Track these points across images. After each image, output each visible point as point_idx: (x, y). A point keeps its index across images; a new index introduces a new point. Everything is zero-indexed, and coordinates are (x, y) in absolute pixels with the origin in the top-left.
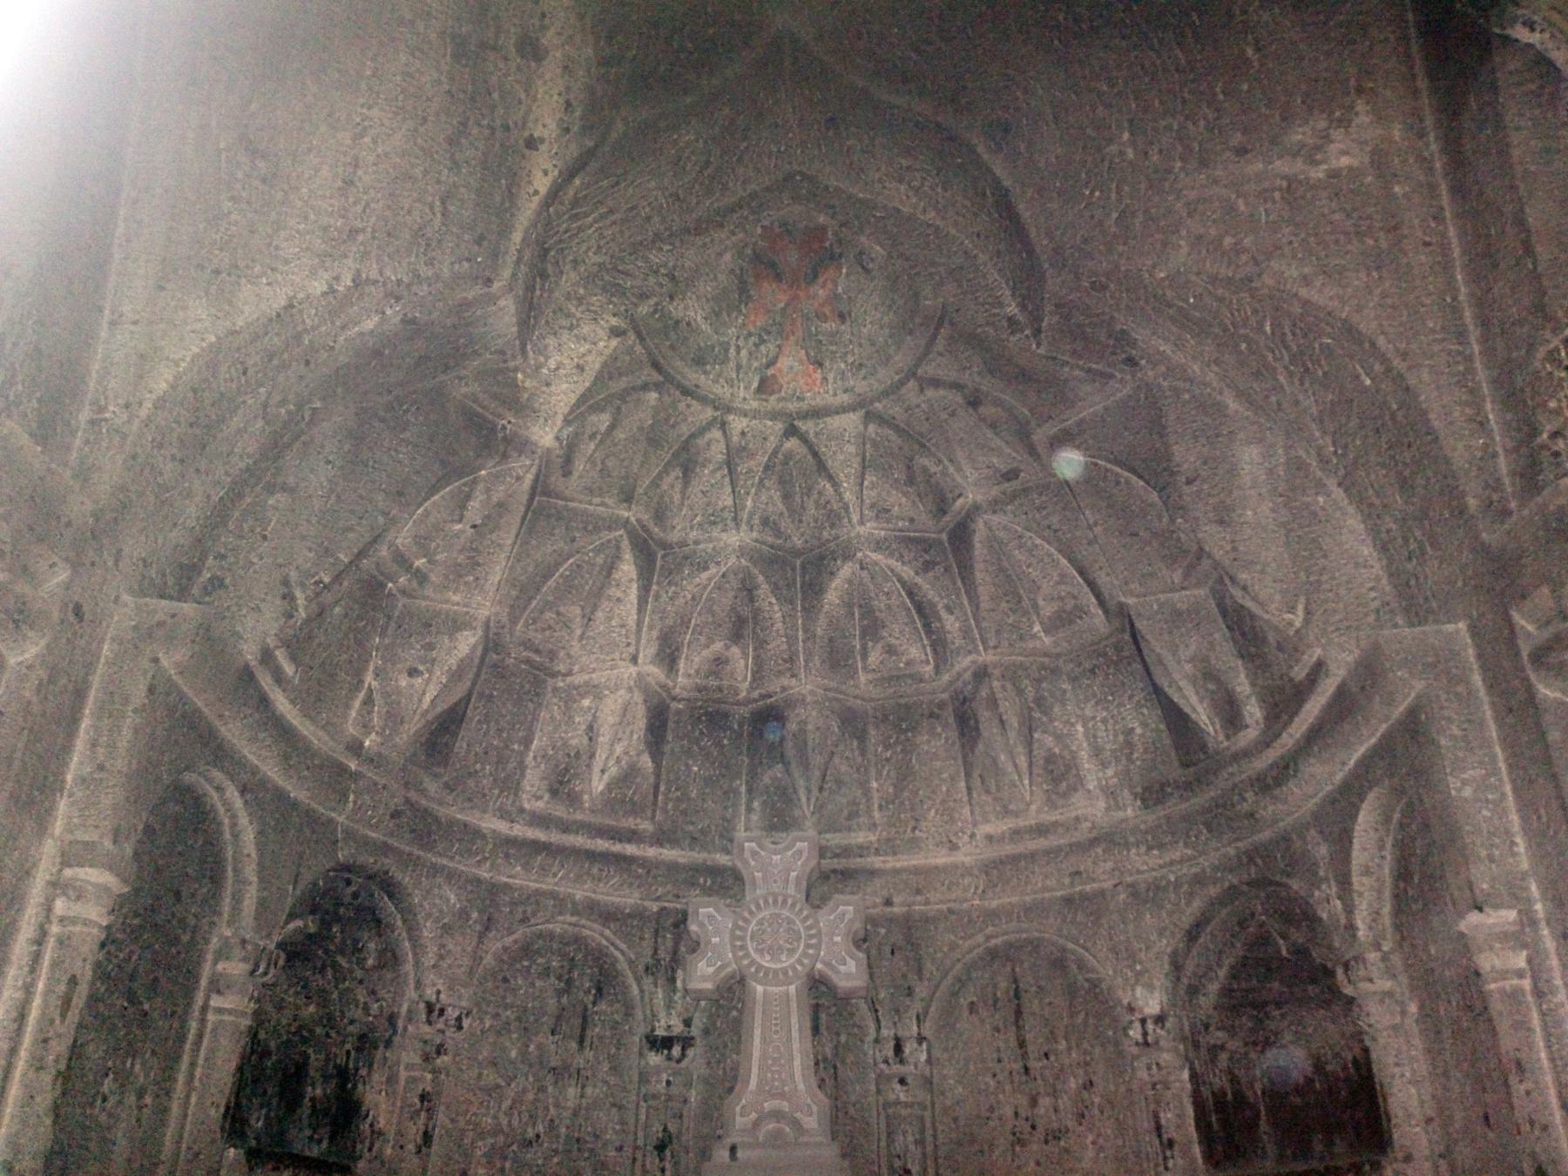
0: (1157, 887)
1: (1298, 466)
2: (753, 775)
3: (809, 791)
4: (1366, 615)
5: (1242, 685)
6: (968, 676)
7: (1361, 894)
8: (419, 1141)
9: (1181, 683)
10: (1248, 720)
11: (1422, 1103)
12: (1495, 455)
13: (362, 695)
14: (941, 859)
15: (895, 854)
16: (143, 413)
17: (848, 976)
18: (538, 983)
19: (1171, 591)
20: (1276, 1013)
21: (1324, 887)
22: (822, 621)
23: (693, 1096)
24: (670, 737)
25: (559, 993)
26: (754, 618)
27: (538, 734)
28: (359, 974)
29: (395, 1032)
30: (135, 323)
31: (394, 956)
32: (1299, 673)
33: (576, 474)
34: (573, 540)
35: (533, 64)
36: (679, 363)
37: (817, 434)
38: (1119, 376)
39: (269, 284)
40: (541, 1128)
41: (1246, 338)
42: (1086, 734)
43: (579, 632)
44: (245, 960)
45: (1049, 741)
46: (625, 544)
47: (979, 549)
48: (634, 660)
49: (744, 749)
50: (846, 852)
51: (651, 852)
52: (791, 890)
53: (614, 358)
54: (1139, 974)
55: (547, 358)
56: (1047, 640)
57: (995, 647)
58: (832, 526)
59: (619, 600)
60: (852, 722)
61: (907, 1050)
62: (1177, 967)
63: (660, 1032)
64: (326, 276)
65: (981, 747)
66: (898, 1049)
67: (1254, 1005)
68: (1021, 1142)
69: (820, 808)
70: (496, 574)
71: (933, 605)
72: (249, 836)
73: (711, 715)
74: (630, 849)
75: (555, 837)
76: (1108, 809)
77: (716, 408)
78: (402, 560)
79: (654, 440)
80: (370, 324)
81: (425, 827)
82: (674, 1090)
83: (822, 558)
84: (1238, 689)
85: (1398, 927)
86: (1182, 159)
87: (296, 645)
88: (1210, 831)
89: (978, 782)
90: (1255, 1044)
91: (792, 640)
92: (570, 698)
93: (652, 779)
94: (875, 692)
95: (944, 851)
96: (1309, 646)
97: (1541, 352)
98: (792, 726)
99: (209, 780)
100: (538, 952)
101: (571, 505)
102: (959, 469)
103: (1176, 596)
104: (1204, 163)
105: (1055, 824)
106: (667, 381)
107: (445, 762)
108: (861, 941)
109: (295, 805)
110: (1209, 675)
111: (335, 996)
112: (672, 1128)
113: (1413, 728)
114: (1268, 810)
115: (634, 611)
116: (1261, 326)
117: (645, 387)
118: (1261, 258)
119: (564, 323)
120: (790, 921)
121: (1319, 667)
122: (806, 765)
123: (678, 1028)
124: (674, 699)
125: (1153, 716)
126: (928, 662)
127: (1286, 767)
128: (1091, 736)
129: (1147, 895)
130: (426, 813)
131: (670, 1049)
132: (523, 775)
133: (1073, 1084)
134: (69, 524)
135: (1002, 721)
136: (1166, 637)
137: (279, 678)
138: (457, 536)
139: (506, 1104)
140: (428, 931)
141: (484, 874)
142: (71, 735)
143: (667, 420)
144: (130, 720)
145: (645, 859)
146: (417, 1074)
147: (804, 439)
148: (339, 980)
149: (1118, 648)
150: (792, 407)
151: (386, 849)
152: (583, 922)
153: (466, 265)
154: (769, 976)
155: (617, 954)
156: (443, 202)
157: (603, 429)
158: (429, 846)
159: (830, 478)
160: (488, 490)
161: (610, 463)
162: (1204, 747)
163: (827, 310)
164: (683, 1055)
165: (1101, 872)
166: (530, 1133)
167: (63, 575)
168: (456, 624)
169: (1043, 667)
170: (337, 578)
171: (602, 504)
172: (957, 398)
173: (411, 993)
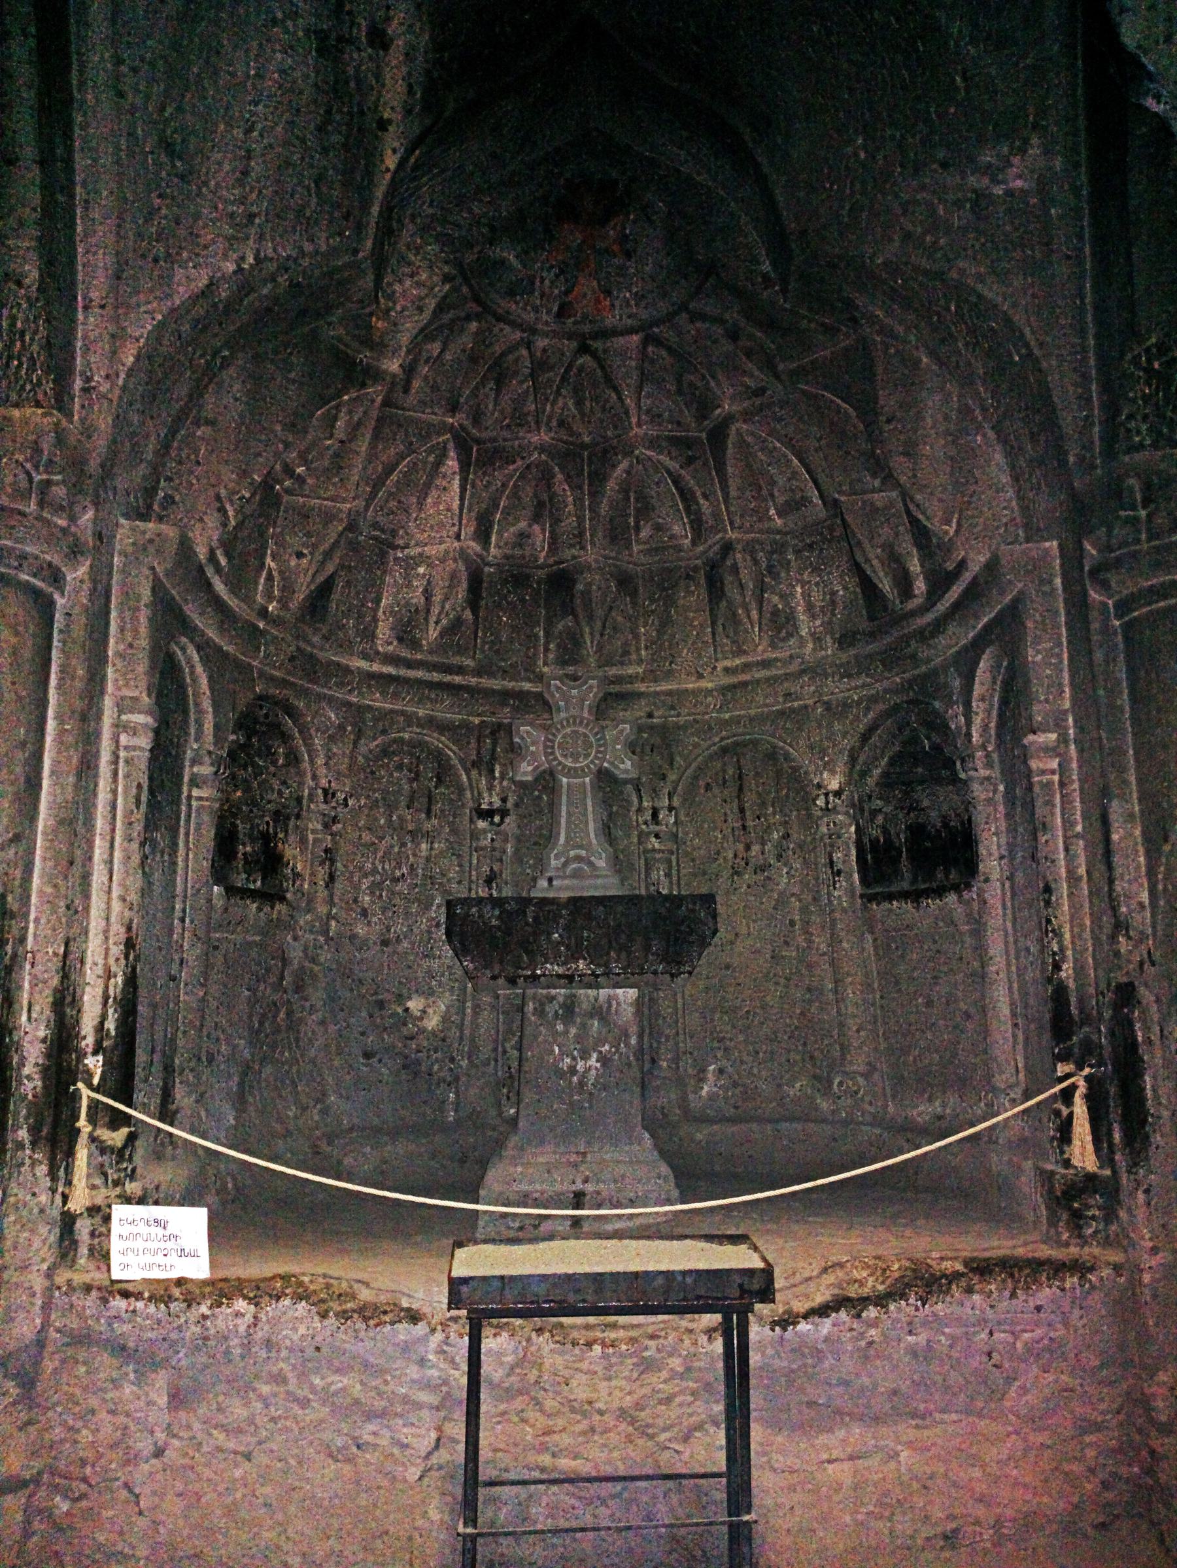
0: (846, 705)
1: (965, 411)
2: (550, 623)
3: (591, 634)
4: (998, 528)
6: (716, 548)
9: (875, 562)
12: (1092, 424)
16: (120, 382)
17: (626, 771)
23: (509, 849)
25: (411, 781)
26: (551, 499)
28: (272, 769)
32: (950, 566)
35: (381, 53)
36: (493, 295)
40: (405, 870)
44: (212, 764)
45: (775, 599)
46: (451, 445)
48: (458, 537)
49: (542, 602)
50: (619, 680)
52: (586, 715)
53: (445, 297)
55: (395, 303)
56: (779, 522)
58: (616, 427)
60: (625, 582)
62: (853, 760)
65: (724, 604)
66: (655, 815)
67: (904, 784)
68: (737, 873)
69: (600, 648)
71: (693, 493)
72: (204, 682)
73: (516, 576)
74: (458, 679)
75: (403, 672)
76: (814, 650)
77: (523, 331)
78: (289, 471)
79: (474, 359)
81: (311, 667)
82: (496, 844)
83: (605, 452)
85: (998, 736)
86: (901, 166)
88: (884, 666)
90: (902, 808)
91: (580, 520)
92: (409, 564)
93: (472, 627)
94: (643, 559)
97: (1129, 356)
98: (580, 587)
99: (177, 643)
102: (718, 384)
105: (776, 660)
107: (323, 620)
108: (632, 747)
109: (226, 655)
111: (255, 784)
112: (495, 868)
114: (924, 653)
117: (468, 318)
119: (407, 270)
120: (585, 735)
122: (591, 618)
123: (497, 803)
125: (853, 582)
127: (939, 626)
128: (806, 595)
129: (836, 710)
130: (311, 656)
133: (775, 835)
135: (741, 585)
137: (218, 570)
138: (328, 448)
139: (380, 854)
142: (107, 624)
150: (587, 328)
151: (284, 683)
154: (571, 772)
156: (317, 186)
158: (315, 681)
159: (615, 389)
160: (350, 412)
162: (885, 608)
163: (615, 248)
164: (502, 821)
166: (398, 873)
167: (90, 514)
169: (775, 542)
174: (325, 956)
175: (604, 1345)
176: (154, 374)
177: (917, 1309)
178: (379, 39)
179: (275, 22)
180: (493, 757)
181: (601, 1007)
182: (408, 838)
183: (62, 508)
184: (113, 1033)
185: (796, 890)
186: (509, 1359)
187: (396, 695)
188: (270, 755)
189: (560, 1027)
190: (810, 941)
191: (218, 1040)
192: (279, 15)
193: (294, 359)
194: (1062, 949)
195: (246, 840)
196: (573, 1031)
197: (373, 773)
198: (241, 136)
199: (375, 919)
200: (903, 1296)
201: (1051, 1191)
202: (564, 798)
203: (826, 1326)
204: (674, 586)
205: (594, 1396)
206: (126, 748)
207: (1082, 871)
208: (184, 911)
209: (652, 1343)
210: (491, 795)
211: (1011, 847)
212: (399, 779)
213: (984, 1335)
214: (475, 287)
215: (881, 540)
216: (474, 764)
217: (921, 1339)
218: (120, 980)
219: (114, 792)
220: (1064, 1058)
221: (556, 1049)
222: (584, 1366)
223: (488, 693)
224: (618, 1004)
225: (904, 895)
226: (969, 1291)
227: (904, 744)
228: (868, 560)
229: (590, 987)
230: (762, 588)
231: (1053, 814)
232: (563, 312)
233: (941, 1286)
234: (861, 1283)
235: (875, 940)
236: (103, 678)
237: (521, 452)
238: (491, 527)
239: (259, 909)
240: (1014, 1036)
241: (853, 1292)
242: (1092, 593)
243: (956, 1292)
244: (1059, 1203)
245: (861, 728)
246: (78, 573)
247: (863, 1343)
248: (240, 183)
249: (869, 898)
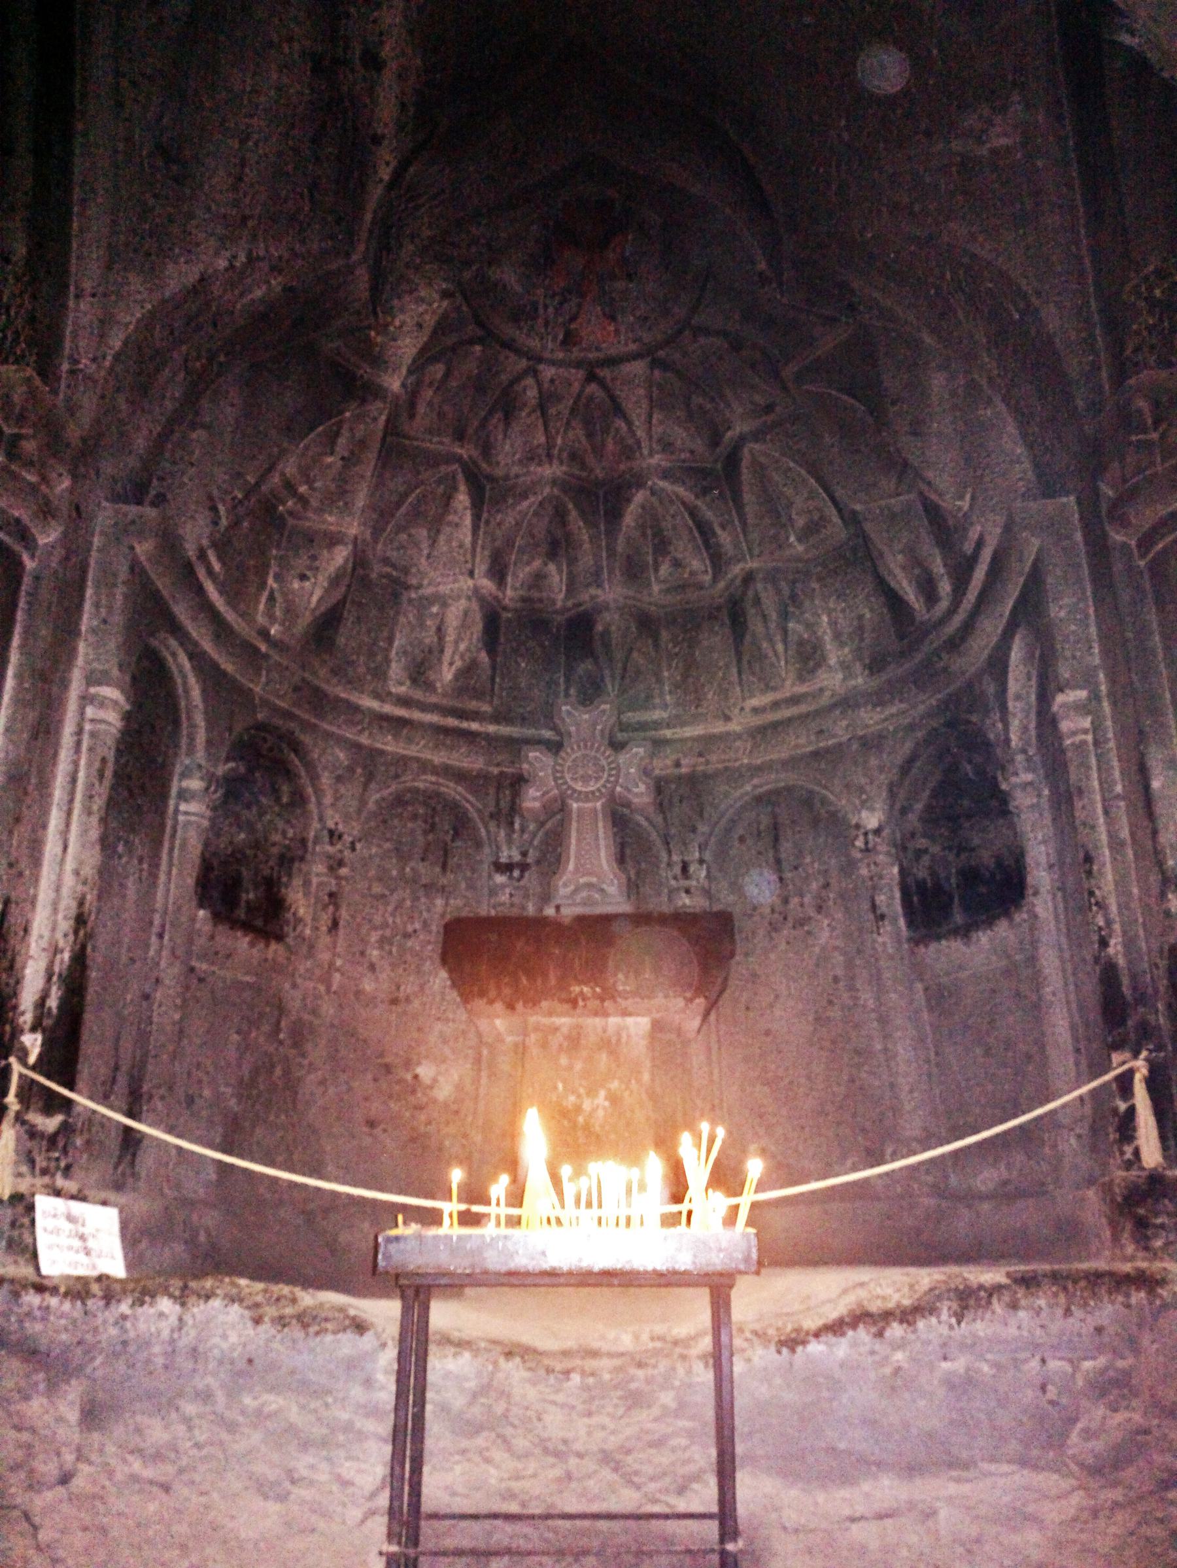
0: (881, 736)
1: (972, 385)
3: (613, 677)
5: (938, 567)
6: (738, 582)
7: (1014, 715)
8: (330, 923)
11: (1048, 854)
12: (1099, 369)
13: (266, 594)
14: (719, 728)
16: (107, 364)
18: (410, 825)
19: (890, 496)
20: (967, 825)
22: (621, 540)
24: (502, 640)
25: (425, 833)
27: (398, 635)
29: (306, 851)
30: (94, 295)
31: (301, 796)
32: (968, 548)
33: (418, 418)
34: (418, 473)
37: (613, 379)
40: (417, 926)
42: (829, 623)
43: (425, 552)
44: (202, 779)
45: (800, 628)
46: (460, 477)
47: (746, 475)
48: (471, 574)
51: (491, 728)
53: (445, 316)
54: (863, 802)
55: (393, 318)
56: (800, 548)
59: (457, 525)
60: (646, 623)
61: (692, 869)
62: (892, 795)
63: (503, 860)
64: (228, 254)
65: (748, 638)
66: (685, 868)
67: (949, 818)
68: (776, 930)
70: (361, 500)
71: (709, 524)
72: (196, 693)
73: (533, 619)
74: (474, 726)
76: (844, 679)
77: (529, 359)
78: (290, 486)
80: (258, 293)
81: (319, 701)
83: (619, 488)
87: (222, 545)
93: (489, 672)
96: (972, 524)
97: (1128, 287)
98: (599, 628)
100: (407, 803)
101: (415, 443)
103: (893, 501)
106: (488, 336)
109: (224, 674)
110: (916, 562)
113: (1035, 578)
115: (469, 534)
116: (943, 277)
117: (471, 342)
118: (941, 219)
123: (517, 858)
124: (505, 608)
128: (833, 623)
129: (871, 743)
131: (511, 871)
132: (389, 666)
133: (814, 886)
134: (68, 445)
135: (764, 616)
136: (885, 535)
137: (210, 572)
138: (329, 466)
139: (390, 908)
140: (326, 779)
141: (364, 740)
143: (489, 370)
144: (120, 591)
145: (488, 734)
146: (325, 879)
147: (602, 383)
148: (261, 814)
149: (854, 550)
150: (591, 355)
152: (441, 781)
157: (439, 376)
160: (351, 429)
161: (446, 408)
164: (522, 877)
165: (840, 730)
166: (410, 929)
167: (66, 483)
168: (333, 540)
170: (247, 496)
171: (441, 443)
172: (718, 341)
173: (316, 825)
174: (328, 1009)
175: (583, 1373)
176: (141, 366)
177: (951, 1327)
178: (373, 62)
179: (271, 44)
181: (609, 1041)
182: (421, 893)
183: (32, 463)
184: (55, 1011)
185: (838, 943)
186: (472, 1384)
187: (410, 740)
188: (276, 792)
189: (564, 1061)
190: (857, 998)
191: (200, 1082)
192: (276, 39)
194: (1109, 923)
195: (251, 887)
196: (578, 1066)
197: (385, 822)
198: (237, 146)
199: (384, 976)
200: (933, 1310)
201: (1113, 1201)
202: (574, 825)
203: (841, 1348)
204: (698, 627)
205: (570, 1435)
206: (92, 721)
207: (1125, 834)
208: (163, 926)
209: (641, 1373)
210: (510, 848)
211: (1060, 853)
212: (413, 831)
213: (1035, 1363)
214: (481, 317)
215: (900, 546)
216: (492, 816)
217: (958, 1365)
218: (66, 956)
219: (76, 763)
220: (1117, 1046)
221: (560, 1086)
222: (560, 1398)
224: (629, 1036)
225: (956, 932)
226: (1014, 1306)
228: (890, 572)
229: (596, 1014)
230: (785, 616)
231: (1088, 778)
232: (569, 339)
233: (978, 1299)
234: (884, 1298)
235: (926, 989)
236: (73, 652)
239: (252, 944)
240: (1077, 1064)
241: (875, 1307)
242: (1112, 534)
243: (997, 1306)
244: (1121, 1214)
245: (899, 759)
246: (48, 536)
247: (888, 1371)
248: (235, 188)
249: (916, 942)
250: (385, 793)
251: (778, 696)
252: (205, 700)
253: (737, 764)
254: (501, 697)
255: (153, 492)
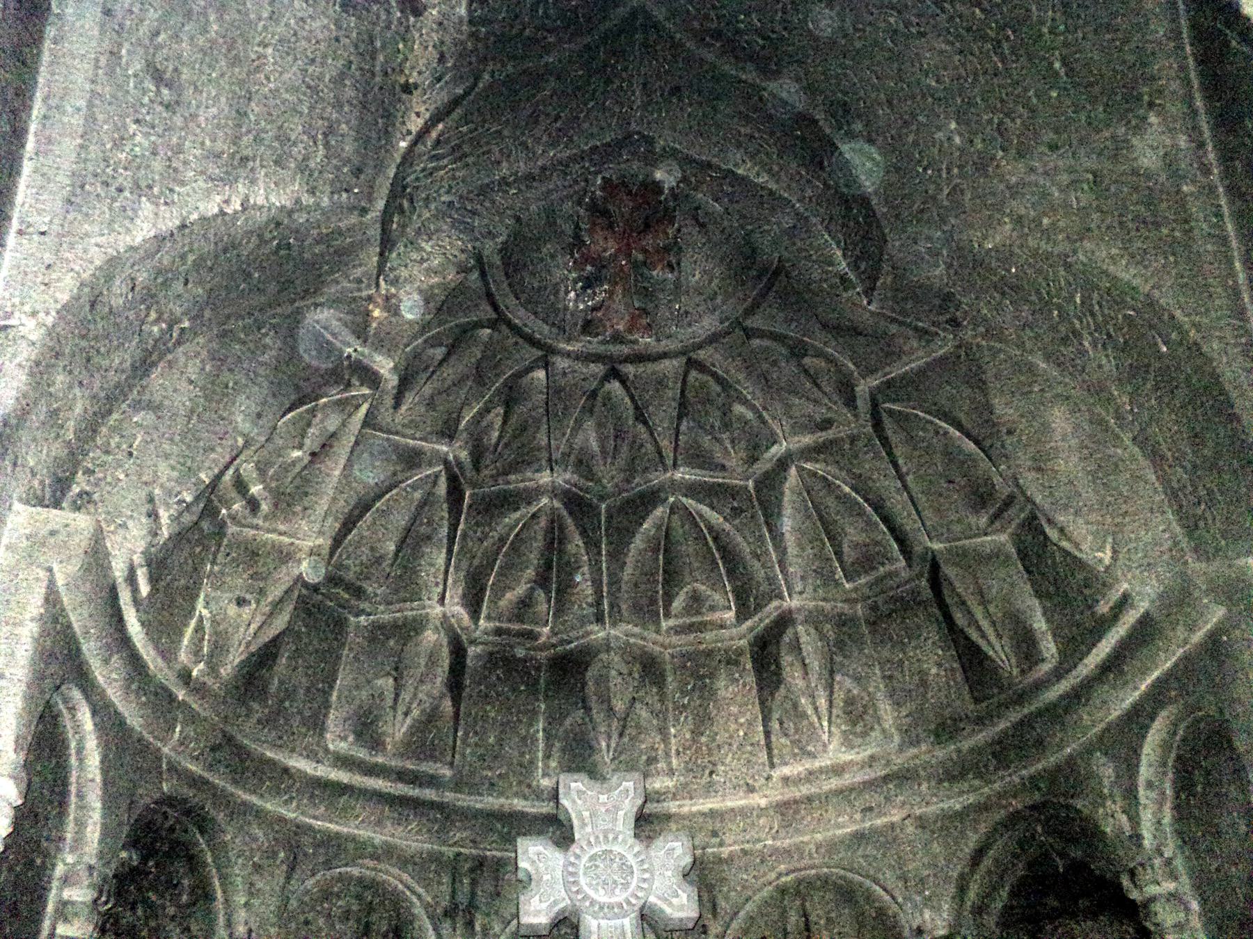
5: (1040, 624)
7: (1145, 806)
10: (1046, 655)
13: (193, 623)
15: (691, 798)
17: (681, 908)
21: (1109, 803)
28: (171, 910)
32: (1103, 608)
38: (942, 334)
39: (166, 203)
41: (1059, 307)
45: (848, 683)
48: (442, 600)
52: (620, 826)
57: (801, 593)
60: (649, 669)
62: (962, 890)
72: (94, 760)
74: (429, 794)
75: (358, 780)
78: (240, 485)
84: (1036, 626)
88: (999, 762)
89: (776, 726)
95: (741, 794)
104: (1021, 155)
117: (479, 325)
119: (415, 256)
121: (1125, 602)
126: (730, 608)
132: (326, 715)
135: (805, 665)
140: (238, 872)
153: (345, 195)
154: (605, 910)
155: (414, 899)
159: (645, 423)
180: (472, 907)
187: (345, 814)
193: (268, 340)
204: (712, 676)
216: (450, 913)
223: (468, 815)
227: (1030, 865)
237: (529, 496)
238: (483, 590)
250: (310, 883)
251: (817, 764)
252: (105, 771)
253: (759, 846)
254: (463, 755)
255: (76, 489)
